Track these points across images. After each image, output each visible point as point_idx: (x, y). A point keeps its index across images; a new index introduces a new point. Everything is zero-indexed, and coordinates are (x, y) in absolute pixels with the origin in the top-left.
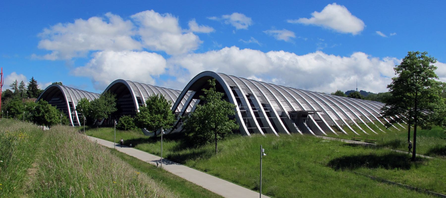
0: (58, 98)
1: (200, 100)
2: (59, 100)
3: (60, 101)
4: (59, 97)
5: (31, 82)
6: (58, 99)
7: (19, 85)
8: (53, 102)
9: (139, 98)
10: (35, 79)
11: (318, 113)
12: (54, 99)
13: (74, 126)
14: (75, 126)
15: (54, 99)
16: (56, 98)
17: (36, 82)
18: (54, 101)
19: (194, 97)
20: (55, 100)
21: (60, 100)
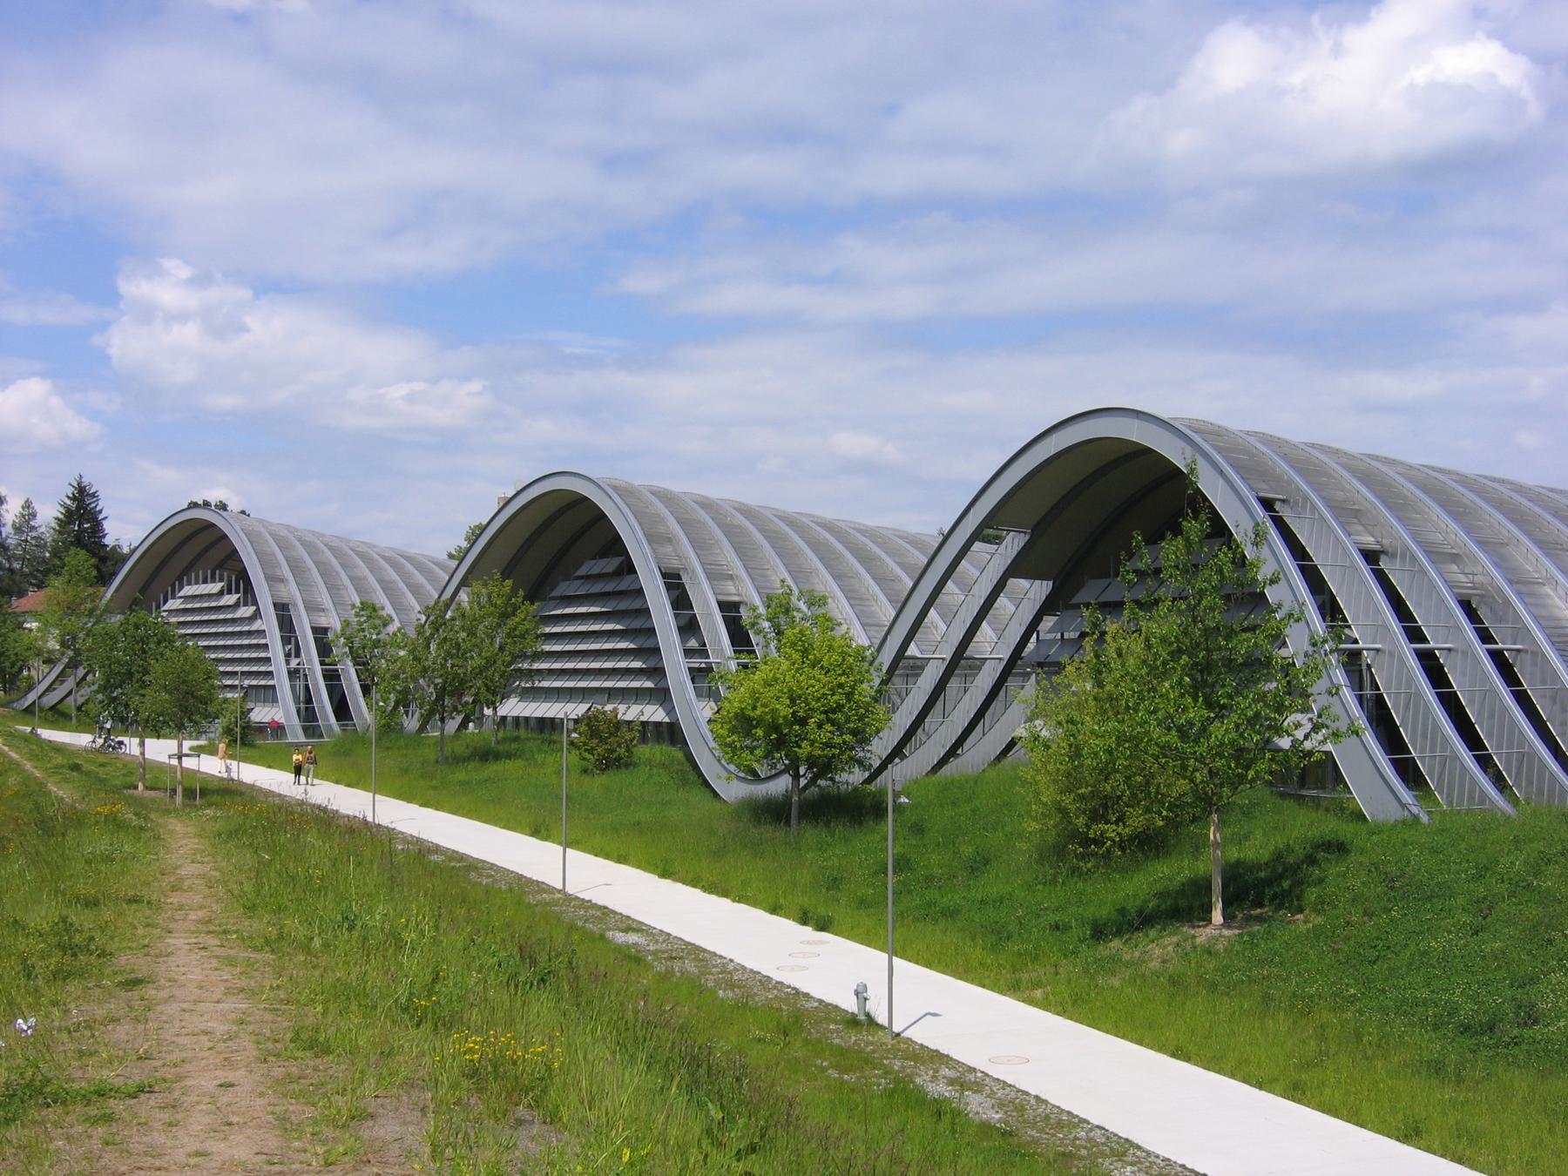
0: (213, 581)
1: (1051, 583)
2: (221, 593)
3: (230, 599)
4: (221, 580)
5: (74, 498)
6: (215, 587)
8: (189, 606)
10: (95, 483)
13: (303, 739)
14: (307, 736)
15: (188, 590)
16: (205, 582)
17: (94, 495)
18: (194, 597)
21: (229, 592)
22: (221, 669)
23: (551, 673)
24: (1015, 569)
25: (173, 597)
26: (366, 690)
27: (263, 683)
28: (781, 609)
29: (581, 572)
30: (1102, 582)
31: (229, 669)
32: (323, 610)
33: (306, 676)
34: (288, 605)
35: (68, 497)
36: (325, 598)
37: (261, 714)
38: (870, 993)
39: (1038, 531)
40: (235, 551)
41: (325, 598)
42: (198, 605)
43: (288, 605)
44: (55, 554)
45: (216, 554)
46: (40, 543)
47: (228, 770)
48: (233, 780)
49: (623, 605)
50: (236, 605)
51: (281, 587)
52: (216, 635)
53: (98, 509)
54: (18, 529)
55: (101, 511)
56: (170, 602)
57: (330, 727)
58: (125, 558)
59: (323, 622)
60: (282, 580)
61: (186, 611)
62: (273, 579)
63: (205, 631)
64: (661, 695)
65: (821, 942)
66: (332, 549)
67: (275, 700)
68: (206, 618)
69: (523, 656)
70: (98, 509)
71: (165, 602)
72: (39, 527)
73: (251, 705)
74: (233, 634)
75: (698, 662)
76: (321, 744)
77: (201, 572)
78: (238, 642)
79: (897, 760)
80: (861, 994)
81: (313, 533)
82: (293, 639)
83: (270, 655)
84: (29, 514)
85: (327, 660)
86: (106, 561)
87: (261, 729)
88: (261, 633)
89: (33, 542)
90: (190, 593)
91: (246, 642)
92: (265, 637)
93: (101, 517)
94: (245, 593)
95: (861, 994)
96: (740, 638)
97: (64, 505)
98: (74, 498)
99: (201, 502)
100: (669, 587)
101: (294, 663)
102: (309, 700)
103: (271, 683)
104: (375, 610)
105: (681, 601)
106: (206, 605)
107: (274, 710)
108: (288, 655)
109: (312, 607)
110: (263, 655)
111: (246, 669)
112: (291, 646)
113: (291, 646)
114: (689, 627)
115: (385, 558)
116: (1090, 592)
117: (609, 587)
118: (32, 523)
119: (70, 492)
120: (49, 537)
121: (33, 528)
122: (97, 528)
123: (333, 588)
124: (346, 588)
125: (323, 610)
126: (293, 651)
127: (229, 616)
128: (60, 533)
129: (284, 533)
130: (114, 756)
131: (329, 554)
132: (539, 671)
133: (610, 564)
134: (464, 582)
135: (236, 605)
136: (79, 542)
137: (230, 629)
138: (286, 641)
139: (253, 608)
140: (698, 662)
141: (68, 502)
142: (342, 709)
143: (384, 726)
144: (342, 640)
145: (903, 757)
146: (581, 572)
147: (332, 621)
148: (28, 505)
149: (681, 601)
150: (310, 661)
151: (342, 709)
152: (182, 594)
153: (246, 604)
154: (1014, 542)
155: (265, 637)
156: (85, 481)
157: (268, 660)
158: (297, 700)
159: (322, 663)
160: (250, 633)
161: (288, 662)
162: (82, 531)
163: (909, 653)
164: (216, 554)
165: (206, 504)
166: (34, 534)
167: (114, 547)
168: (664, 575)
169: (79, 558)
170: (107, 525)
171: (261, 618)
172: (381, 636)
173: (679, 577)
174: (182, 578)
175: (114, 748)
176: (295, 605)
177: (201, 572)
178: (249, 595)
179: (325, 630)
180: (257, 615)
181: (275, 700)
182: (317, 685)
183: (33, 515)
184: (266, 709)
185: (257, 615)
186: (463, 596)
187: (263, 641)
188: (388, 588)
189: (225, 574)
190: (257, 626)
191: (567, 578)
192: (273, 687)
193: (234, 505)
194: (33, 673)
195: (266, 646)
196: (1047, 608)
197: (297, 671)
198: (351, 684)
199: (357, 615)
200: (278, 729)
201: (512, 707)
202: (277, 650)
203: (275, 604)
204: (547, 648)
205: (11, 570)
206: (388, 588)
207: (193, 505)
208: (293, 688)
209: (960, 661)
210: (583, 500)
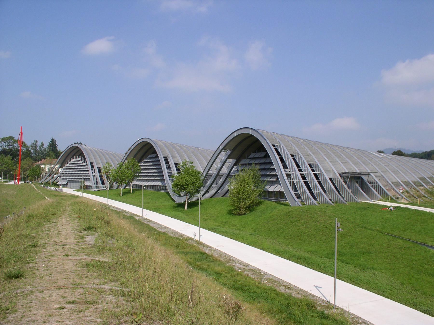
0: (78, 158)
3: (81, 162)
4: (80, 158)
6: (79, 159)
7: (39, 144)
8: (74, 163)
9: (167, 158)
10: (55, 138)
11: (372, 174)
12: (73, 160)
15: (73, 160)
16: (77, 158)
17: (55, 141)
19: (229, 157)
21: (81, 160)
23: (142, 176)
24: (229, 157)
27: (88, 178)
28: (184, 165)
29: (149, 157)
30: (245, 160)
31: (81, 175)
37: (87, 184)
38: (196, 234)
39: (233, 150)
40: (83, 152)
41: (100, 162)
44: (48, 152)
45: (79, 153)
46: (44, 151)
47: (81, 194)
49: (156, 163)
56: (70, 162)
58: (62, 153)
64: (163, 180)
65: (189, 226)
67: (90, 180)
69: (137, 173)
71: (69, 162)
75: (170, 174)
79: (207, 193)
80: (195, 236)
83: (89, 172)
84: (42, 144)
85: (100, 173)
86: (57, 154)
87: (87, 187)
95: (195, 236)
96: (178, 170)
98: (51, 142)
99: (76, 143)
100: (165, 160)
101: (94, 174)
102: (97, 181)
103: (89, 178)
105: (167, 162)
114: (169, 168)
116: (242, 162)
117: (154, 160)
119: (51, 140)
121: (43, 148)
132: (140, 176)
133: (154, 156)
134: (126, 159)
135: (83, 163)
136: (52, 150)
139: (86, 163)
140: (170, 174)
141: (50, 142)
142: (103, 183)
144: (103, 169)
145: (209, 192)
146: (149, 157)
147: (101, 166)
148: (42, 143)
149: (167, 162)
150: (97, 174)
151: (103, 183)
153: (85, 163)
154: (229, 152)
156: (54, 138)
159: (99, 174)
162: (53, 148)
163: (209, 173)
164: (79, 153)
165: (78, 143)
168: (164, 158)
169: (52, 153)
170: (58, 147)
173: (167, 158)
174: (73, 156)
178: (85, 161)
179: (100, 168)
183: (43, 145)
186: (126, 161)
187: (88, 170)
188: (112, 160)
190: (87, 167)
191: (146, 158)
193: (83, 143)
195: (88, 171)
196: (235, 164)
197: (94, 175)
199: (106, 165)
200: (91, 187)
201: (135, 183)
204: (142, 171)
207: (75, 143)
209: (218, 175)
210: (149, 143)
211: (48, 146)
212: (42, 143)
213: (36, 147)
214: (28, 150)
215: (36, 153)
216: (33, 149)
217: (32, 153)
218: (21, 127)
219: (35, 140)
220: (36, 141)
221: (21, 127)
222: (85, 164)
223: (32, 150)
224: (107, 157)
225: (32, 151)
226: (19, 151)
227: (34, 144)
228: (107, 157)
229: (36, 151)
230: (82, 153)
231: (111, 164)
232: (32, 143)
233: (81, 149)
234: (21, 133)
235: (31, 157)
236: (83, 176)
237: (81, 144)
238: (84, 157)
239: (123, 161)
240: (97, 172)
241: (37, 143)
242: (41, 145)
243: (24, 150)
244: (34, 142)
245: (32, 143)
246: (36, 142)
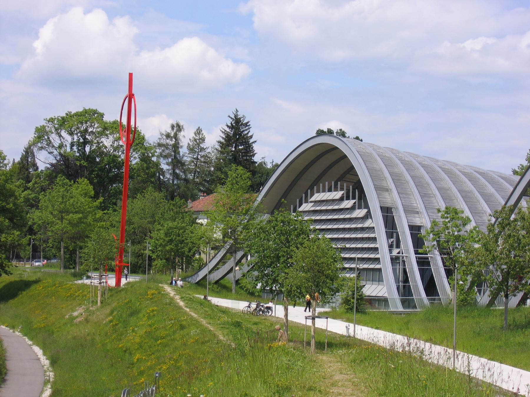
0: (336, 189)
2: (341, 199)
3: (348, 204)
4: (342, 189)
8: (318, 208)
10: (247, 115)
13: (401, 309)
14: (404, 307)
15: (317, 197)
16: (330, 190)
17: (246, 125)
18: (321, 202)
20: (330, 198)
21: (348, 198)
22: (343, 255)
25: (306, 202)
26: (449, 273)
27: (372, 266)
32: (418, 213)
33: (404, 262)
34: (391, 208)
35: (228, 126)
36: (419, 204)
40: (352, 168)
41: (419, 204)
42: (324, 208)
43: (391, 208)
44: (218, 168)
45: (338, 170)
48: (349, 336)
50: (353, 208)
51: (386, 194)
52: (338, 230)
53: (249, 135)
54: (191, 150)
55: (251, 137)
57: (421, 300)
59: (417, 221)
60: (387, 190)
61: (315, 212)
62: (380, 189)
63: (330, 227)
66: (424, 166)
67: (380, 280)
68: (330, 217)
70: (249, 135)
71: (301, 205)
72: (207, 148)
73: (362, 283)
74: (350, 230)
76: (416, 313)
77: (327, 183)
78: (353, 236)
81: (410, 154)
82: (395, 235)
83: (377, 246)
85: (420, 251)
88: (371, 229)
89: (202, 159)
90: (318, 199)
91: (360, 236)
92: (374, 232)
93: (251, 141)
94: (360, 199)
97: (225, 132)
98: (231, 127)
101: (395, 252)
103: (378, 266)
104: (456, 213)
106: (330, 208)
107: (380, 287)
108: (391, 246)
109: (409, 211)
110: (372, 246)
111: (360, 256)
112: (394, 240)
113: (394, 240)
115: (464, 174)
118: (202, 145)
119: (229, 122)
120: (213, 156)
121: (203, 149)
122: (249, 150)
123: (425, 196)
124: (435, 196)
125: (418, 213)
126: (395, 243)
127: (348, 216)
128: (222, 153)
129: (389, 154)
130: (263, 318)
131: (422, 170)
134: (524, 193)
135: (353, 208)
137: (348, 226)
138: (389, 235)
139: (365, 211)
141: (228, 130)
143: (462, 301)
144: (431, 235)
148: (199, 131)
150: (408, 251)
152: (313, 199)
153: (360, 208)
155: (374, 232)
156: (240, 115)
157: (376, 250)
158: (397, 280)
159: (416, 253)
160: (362, 229)
161: (390, 251)
162: (237, 151)
164: (338, 170)
166: (203, 153)
167: (261, 163)
170: (255, 147)
171: (371, 218)
172: (461, 233)
174: (313, 187)
175: (263, 312)
176: (397, 208)
177: (327, 183)
179: (419, 228)
180: (368, 216)
181: (380, 280)
182: (412, 269)
183: (203, 140)
184: (374, 286)
185: (368, 216)
186: (523, 203)
187: (372, 235)
188: (467, 197)
189: (345, 185)
190: (368, 223)
192: (380, 270)
194: (203, 256)
197: (397, 258)
198: (438, 269)
199: (443, 217)
200: (383, 301)
202: (383, 242)
203: (381, 208)
205: (186, 180)
206: (467, 197)
207: (320, 133)
208: (394, 270)
211: (219, 142)
212: (199, 131)
213: (176, 147)
214: (145, 159)
215: (177, 171)
216: (166, 157)
217: (162, 172)
218: (131, 75)
219: (175, 123)
220: (178, 125)
221: (131, 75)
222: (360, 213)
223: (162, 160)
224: (448, 183)
225: (164, 166)
226: (119, 166)
227: (168, 136)
228: (448, 183)
229: (177, 163)
230: (351, 169)
231: (464, 215)
232: (162, 134)
233: (345, 157)
234: (131, 96)
235: (160, 186)
236: (358, 258)
237: (342, 134)
238: (358, 187)
239: (512, 202)
240: (406, 245)
241: (182, 133)
242: (195, 140)
243: (135, 160)
244: (169, 130)
245: (162, 134)
246: (178, 128)
